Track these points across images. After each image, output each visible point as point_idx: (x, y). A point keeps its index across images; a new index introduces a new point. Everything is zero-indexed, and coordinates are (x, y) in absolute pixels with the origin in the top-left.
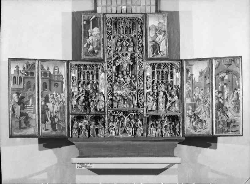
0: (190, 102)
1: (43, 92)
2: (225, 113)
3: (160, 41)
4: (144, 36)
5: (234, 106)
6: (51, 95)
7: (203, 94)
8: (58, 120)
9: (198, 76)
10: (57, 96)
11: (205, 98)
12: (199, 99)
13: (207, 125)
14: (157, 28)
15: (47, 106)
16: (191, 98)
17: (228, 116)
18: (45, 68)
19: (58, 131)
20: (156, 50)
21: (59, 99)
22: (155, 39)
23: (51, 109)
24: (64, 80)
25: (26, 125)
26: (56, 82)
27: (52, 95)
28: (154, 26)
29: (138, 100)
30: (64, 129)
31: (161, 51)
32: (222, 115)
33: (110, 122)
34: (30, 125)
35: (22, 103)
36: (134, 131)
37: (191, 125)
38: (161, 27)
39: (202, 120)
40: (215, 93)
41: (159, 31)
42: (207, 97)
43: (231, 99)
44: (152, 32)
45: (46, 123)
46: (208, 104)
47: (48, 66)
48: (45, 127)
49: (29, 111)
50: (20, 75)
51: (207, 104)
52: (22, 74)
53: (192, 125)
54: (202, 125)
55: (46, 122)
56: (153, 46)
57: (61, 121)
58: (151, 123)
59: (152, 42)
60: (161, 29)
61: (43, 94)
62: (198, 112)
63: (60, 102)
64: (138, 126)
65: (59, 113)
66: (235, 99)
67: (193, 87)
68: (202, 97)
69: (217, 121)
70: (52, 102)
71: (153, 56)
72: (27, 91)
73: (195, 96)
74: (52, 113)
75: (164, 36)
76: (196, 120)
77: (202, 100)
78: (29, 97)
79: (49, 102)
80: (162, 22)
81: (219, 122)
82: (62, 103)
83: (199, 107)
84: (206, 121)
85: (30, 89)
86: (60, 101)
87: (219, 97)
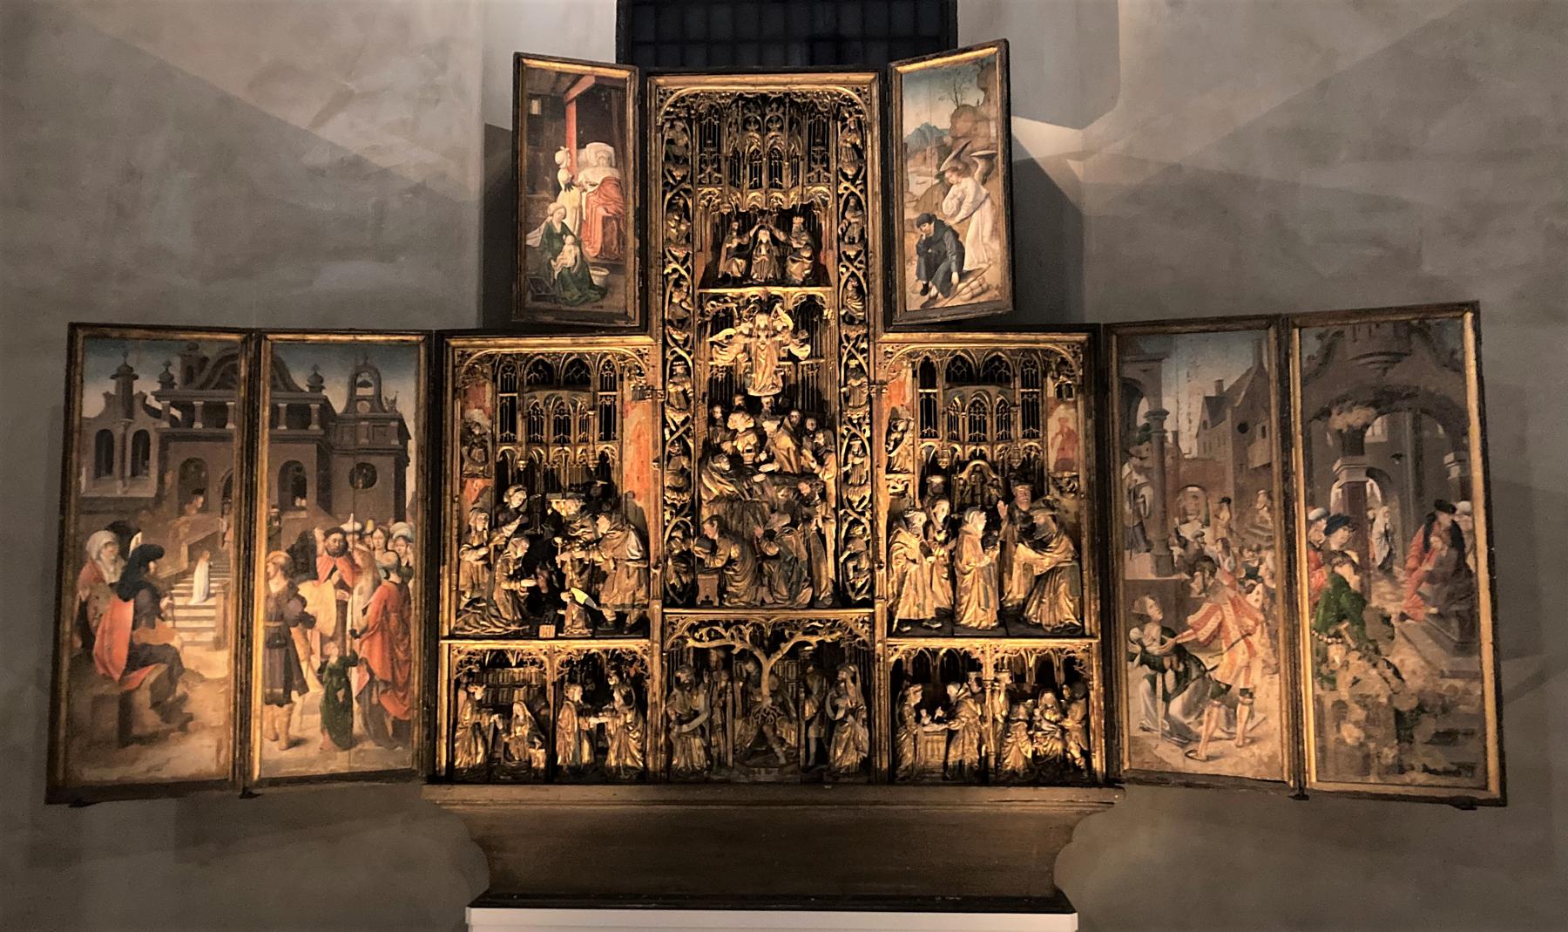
0: (1152, 577)
1: (278, 518)
2: (1377, 651)
3: (962, 215)
4: (874, 194)
5: (1434, 610)
6: (327, 535)
7: (1230, 531)
8: (367, 678)
9: (1196, 423)
10: (367, 539)
11: (1241, 552)
12: (1209, 559)
13: (1259, 716)
14: (948, 140)
15: (303, 602)
16: (1158, 549)
17: (1397, 673)
18: (301, 380)
19: (369, 745)
20: (942, 268)
21: (377, 555)
22: (938, 206)
23: (327, 620)
24: (412, 445)
25: (166, 719)
26: (361, 459)
27: (338, 536)
29: (841, 560)
30: (401, 728)
31: (969, 272)
32: (1357, 664)
33: (676, 691)
34: (191, 718)
35: (148, 586)
36: (818, 740)
37: (1161, 713)
38: (964, 136)
39: (1229, 687)
40: (1309, 523)
41: (955, 157)
42: (1259, 550)
43: (1411, 563)
45: (289, 701)
46: (1267, 589)
47: (315, 368)
48: (288, 725)
49: (186, 636)
50: (142, 421)
51: (1259, 587)
52: (156, 414)
53: (1167, 716)
54: (1231, 720)
55: (294, 694)
56: (926, 245)
57: (386, 683)
58: (915, 695)
59: (920, 223)
60: (966, 145)
61: (279, 530)
62: (1203, 635)
63: (383, 574)
64: (841, 715)
65: (378, 638)
66: (1440, 563)
67: (1169, 488)
68: (1226, 547)
69: (1328, 703)
70: (335, 577)
72: (182, 512)
73: (1179, 537)
74: (332, 639)
75: (984, 182)
76: (1192, 686)
77: (1226, 564)
78: (191, 548)
79: (315, 577)
80: (974, 104)
81: (1340, 705)
82: (394, 577)
83: (1206, 607)
84: (1251, 696)
85: (201, 499)
86: (387, 570)
87: (1334, 553)
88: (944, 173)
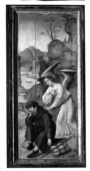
3: (54, 105)
14: (46, 59)
20: (41, 135)
28: (37, 51)
31: (58, 140)
38: (56, 59)
41: (52, 70)
44: (30, 73)
59: (28, 106)
71: (29, 156)
88: (43, 78)
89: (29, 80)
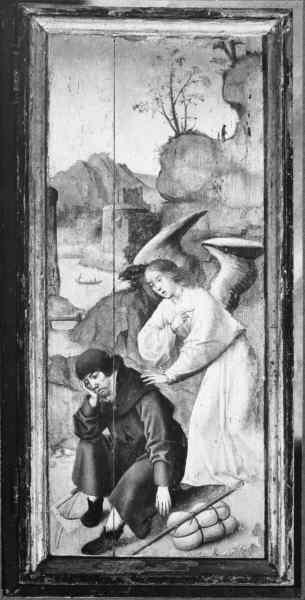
3: (181, 366)
14: (153, 200)
20: (134, 472)
28: (119, 171)
31: (195, 492)
38: (190, 199)
41: (174, 240)
44: (93, 250)
59: (84, 369)
88: (142, 269)
89: (90, 274)
